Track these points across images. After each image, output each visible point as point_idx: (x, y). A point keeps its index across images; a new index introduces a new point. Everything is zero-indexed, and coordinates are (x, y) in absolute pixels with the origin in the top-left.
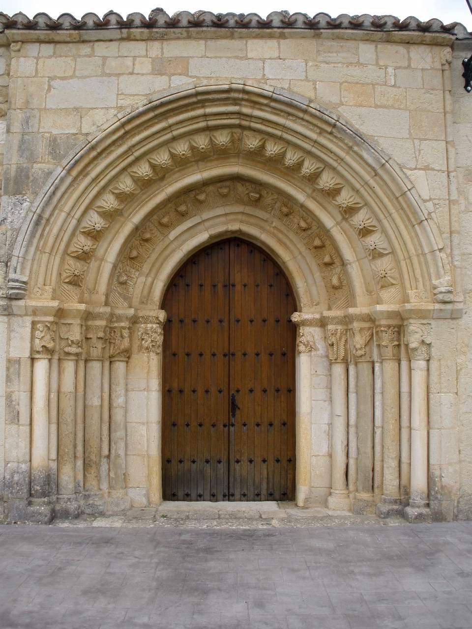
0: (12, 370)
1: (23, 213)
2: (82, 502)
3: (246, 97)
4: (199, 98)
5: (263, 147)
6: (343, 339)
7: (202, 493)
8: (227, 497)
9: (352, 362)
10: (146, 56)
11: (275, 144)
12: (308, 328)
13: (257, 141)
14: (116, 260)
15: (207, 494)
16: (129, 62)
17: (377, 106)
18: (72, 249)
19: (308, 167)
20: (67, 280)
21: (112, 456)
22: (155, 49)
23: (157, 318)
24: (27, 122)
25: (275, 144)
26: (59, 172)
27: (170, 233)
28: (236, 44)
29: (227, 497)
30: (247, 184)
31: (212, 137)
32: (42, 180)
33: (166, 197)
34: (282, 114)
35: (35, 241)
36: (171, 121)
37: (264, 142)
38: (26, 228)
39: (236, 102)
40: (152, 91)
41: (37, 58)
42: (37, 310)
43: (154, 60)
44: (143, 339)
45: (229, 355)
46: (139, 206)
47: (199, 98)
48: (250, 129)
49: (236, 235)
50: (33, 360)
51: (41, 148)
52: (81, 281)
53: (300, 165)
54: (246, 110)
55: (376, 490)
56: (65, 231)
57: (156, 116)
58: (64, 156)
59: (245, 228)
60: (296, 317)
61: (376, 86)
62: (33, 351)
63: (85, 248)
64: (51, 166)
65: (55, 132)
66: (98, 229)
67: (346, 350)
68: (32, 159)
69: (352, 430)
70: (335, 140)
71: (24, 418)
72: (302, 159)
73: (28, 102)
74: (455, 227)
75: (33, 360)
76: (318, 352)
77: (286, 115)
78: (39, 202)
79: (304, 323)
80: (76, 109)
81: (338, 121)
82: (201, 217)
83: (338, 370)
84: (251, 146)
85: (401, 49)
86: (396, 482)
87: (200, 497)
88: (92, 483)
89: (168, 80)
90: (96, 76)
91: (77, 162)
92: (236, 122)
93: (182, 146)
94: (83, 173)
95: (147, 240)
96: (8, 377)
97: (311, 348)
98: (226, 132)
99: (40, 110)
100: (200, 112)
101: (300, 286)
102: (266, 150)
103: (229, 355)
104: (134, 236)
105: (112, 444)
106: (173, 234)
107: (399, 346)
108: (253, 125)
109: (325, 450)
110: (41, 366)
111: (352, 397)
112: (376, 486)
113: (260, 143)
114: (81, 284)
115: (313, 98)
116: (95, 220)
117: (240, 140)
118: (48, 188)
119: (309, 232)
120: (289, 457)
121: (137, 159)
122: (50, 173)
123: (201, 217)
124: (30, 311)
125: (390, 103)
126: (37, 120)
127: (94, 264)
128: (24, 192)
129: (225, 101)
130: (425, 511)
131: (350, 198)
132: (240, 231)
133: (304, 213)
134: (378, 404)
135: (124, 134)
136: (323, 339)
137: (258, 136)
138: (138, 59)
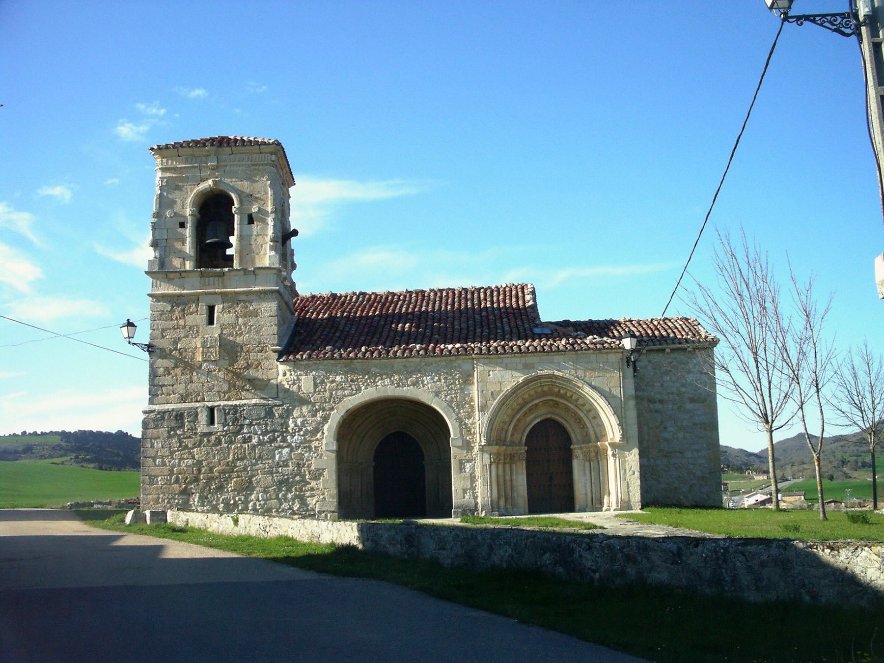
10: (520, 363)
16: (514, 365)
19: (574, 397)
22: (523, 360)
23: (525, 449)
28: (550, 358)
39: (551, 378)
43: (523, 365)
45: (548, 461)
50: (490, 465)
53: (572, 397)
54: (553, 380)
59: (553, 416)
60: (572, 447)
62: (491, 462)
74: (623, 416)
83: (587, 464)
85: (605, 355)
97: (577, 457)
101: (572, 435)
103: (548, 461)
109: (584, 492)
117: (552, 388)
129: (547, 378)
134: (601, 475)
138: (518, 364)
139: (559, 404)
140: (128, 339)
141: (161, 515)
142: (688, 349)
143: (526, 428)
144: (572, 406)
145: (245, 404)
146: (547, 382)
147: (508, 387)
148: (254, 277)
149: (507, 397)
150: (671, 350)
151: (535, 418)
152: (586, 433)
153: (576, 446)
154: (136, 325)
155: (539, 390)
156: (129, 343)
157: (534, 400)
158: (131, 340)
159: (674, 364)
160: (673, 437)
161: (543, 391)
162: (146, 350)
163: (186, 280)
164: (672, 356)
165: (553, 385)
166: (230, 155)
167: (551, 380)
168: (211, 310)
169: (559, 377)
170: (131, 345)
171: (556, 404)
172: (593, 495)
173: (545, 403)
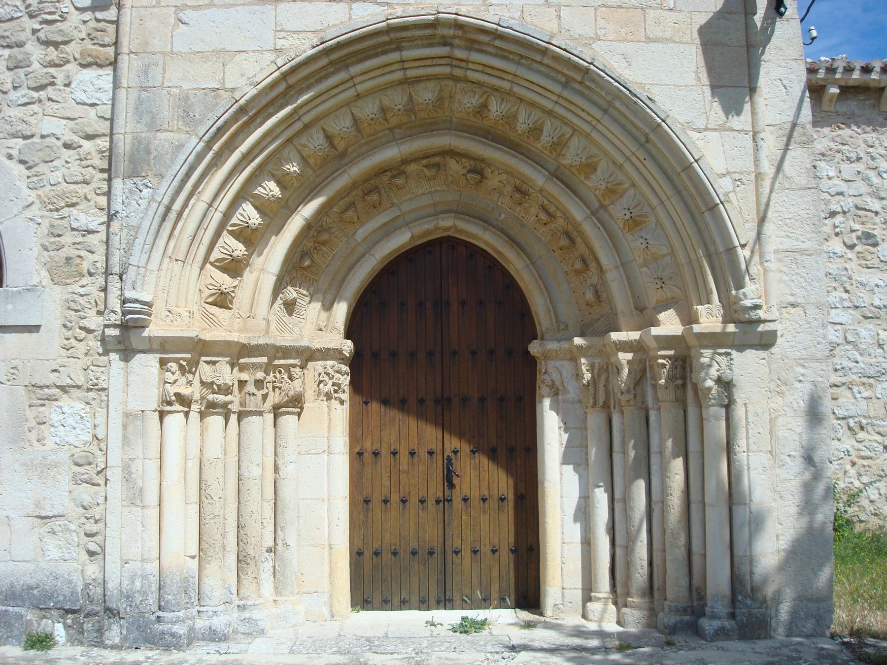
0: (130, 428)
2: (236, 614)
3: (459, 33)
4: (393, 36)
5: (485, 106)
6: (603, 377)
7: (407, 598)
8: (442, 604)
9: (617, 409)
11: (503, 100)
12: (552, 362)
13: (477, 97)
14: (281, 270)
15: (415, 599)
17: (649, 40)
18: (216, 255)
20: (210, 300)
21: (280, 547)
24: (146, 72)
25: (503, 100)
26: (194, 145)
27: (356, 232)
29: (442, 604)
30: (464, 160)
31: (413, 94)
32: (169, 156)
33: (350, 181)
34: (511, 56)
35: (161, 242)
36: (355, 69)
37: (487, 99)
38: (148, 223)
39: (445, 42)
40: (325, 25)
42: (167, 343)
44: (321, 382)
46: (312, 194)
47: (393, 36)
48: (466, 80)
49: (449, 233)
50: (162, 415)
51: (167, 112)
52: (231, 303)
53: (536, 131)
54: (459, 54)
55: (656, 594)
56: (206, 230)
57: (331, 63)
58: (201, 122)
59: (462, 225)
60: (534, 348)
61: (647, 11)
63: (235, 254)
64: (183, 136)
65: (186, 86)
66: (254, 227)
67: (607, 393)
68: (155, 127)
70: (586, 92)
71: (152, 498)
72: (541, 121)
73: (146, 43)
75: (162, 415)
76: (568, 396)
77: (517, 58)
78: (165, 189)
79: (546, 356)
80: (219, 52)
81: (591, 64)
82: (400, 209)
83: (595, 420)
84: (468, 105)
86: (684, 582)
87: (404, 605)
88: (249, 588)
89: (347, 10)
90: (243, 5)
91: (220, 131)
92: (447, 70)
93: (371, 106)
94: (230, 146)
95: (324, 243)
96: (125, 437)
98: (431, 85)
99: (163, 54)
100: (395, 56)
101: (538, 304)
102: (489, 111)
104: (306, 237)
105: (279, 530)
106: (361, 234)
107: (684, 386)
108: (471, 75)
112: (655, 587)
113: (481, 101)
114: (230, 306)
115: (556, 30)
116: (249, 214)
118: (178, 168)
119: (553, 226)
120: (529, 545)
121: (307, 127)
122: (181, 146)
123: (400, 209)
124: (156, 346)
125: (668, 34)
126: (159, 70)
127: (249, 276)
128: (144, 174)
130: (728, 624)
131: (610, 176)
133: (545, 200)
135: (287, 89)
136: (574, 377)
137: (478, 90)
139: (488, 172)
144: (538, 178)
150: (840, 87)
151: (387, 230)
152: (597, 293)
153: (552, 346)
155: (396, 99)
157: (374, 144)
160: (846, 338)
161: (411, 108)
165: (456, 79)
169: (483, 38)
172: (619, 551)
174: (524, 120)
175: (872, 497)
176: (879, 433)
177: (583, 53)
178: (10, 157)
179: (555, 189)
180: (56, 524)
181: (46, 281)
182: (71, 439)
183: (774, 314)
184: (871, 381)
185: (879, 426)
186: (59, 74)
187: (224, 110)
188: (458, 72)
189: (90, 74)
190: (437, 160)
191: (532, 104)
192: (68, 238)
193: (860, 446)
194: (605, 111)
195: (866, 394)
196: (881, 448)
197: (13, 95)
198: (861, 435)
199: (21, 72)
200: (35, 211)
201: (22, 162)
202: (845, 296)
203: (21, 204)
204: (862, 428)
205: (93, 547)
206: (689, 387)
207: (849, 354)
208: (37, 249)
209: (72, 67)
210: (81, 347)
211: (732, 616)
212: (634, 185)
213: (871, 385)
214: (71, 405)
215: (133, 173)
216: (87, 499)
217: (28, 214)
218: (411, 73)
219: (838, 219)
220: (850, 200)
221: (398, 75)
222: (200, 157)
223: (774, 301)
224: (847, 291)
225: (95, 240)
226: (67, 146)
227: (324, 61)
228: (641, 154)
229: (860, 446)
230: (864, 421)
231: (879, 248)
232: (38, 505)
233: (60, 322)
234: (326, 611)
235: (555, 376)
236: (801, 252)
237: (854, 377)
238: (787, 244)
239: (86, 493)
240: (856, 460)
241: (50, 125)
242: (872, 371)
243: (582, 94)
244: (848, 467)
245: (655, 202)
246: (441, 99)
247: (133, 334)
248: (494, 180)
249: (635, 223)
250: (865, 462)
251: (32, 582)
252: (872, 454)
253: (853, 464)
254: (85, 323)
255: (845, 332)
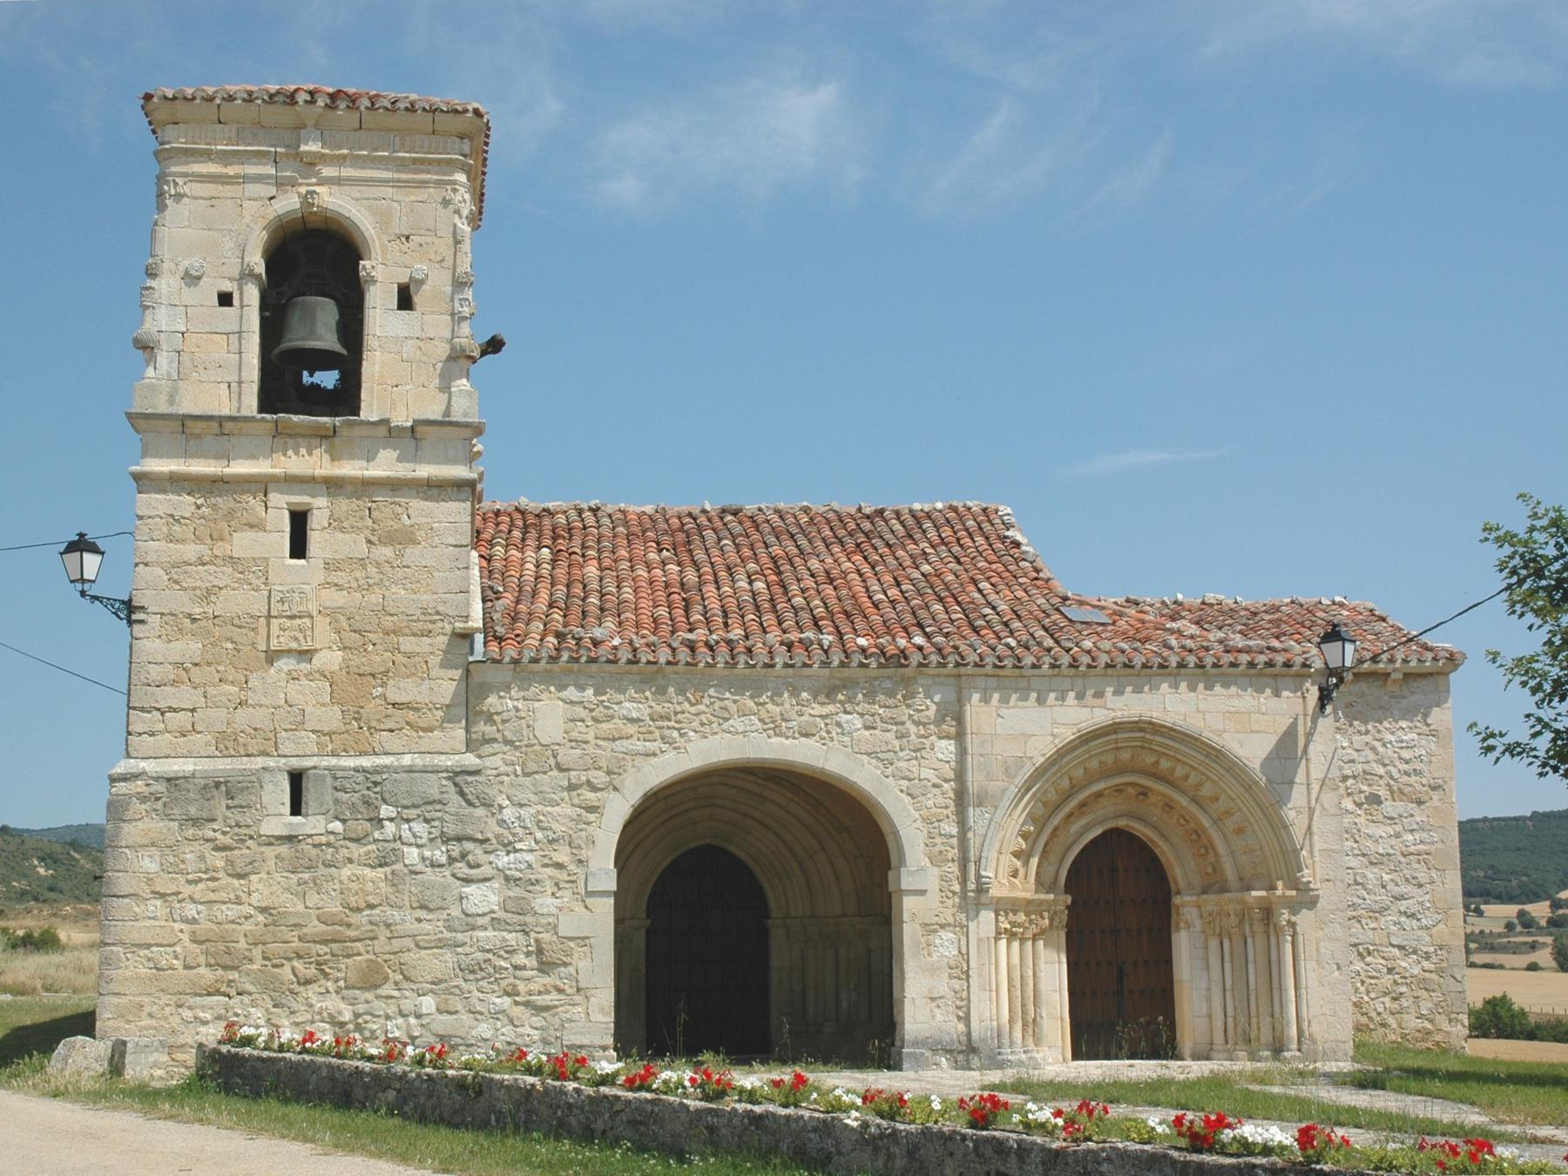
1: (986, 822)
17: (1252, 732)
19: (1193, 779)
39: (1142, 730)
41: (985, 690)
50: (996, 939)
53: (1186, 777)
54: (1148, 736)
59: (1131, 824)
62: (998, 933)
64: (1006, 784)
67: (1221, 928)
69: (1228, 994)
79: (1183, 905)
83: (1214, 943)
97: (1188, 926)
99: (991, 735)
100: (1114, 737)
107: (1268, 924)
110: (1003, 943)
111: (1227, 966)
122: (1005, 789)
125: (1262, 728)
132: (1127, 826)
139: (1150, 794)
140: (79, 586)
141: (157, 1050)
142: (1394, 676)
143: (1068, 849)
144: (1184, 802)
145: (386, 766)
146: (1134, 739)
147: (1041, 749)
148: (413, 443)
149: (1040, 773)
151: (1088, 828)
153: (1187, 898)
154: (102, 550)
155: (1109, 759)
156: (83, 593)
157: (1091, 783)
158: (86, 587)
159: (1359, 708)
161: (1116, 760)
162: (122, 616)
163: (233, 440)
164: (1356, 688)
166: (355, 130)
167: (1142, 734)
168: (299, 521)
169: (1163, 730)
170: (86, 602)
171: (1144, 793)
173: (1118, 790)
174: (1180, 771)
175: (1379, 1010)
176: (1383, 958)
177: (1217, 741)
178: (902, 791)
179: (1193, 809)
180: (940, 1002)
181: (929, 864)
182: (947, 954)
183: (1318, 885)
184: (1376, 915)
185: (1382, 951)
186: (927, 742)
187: (1028, 770)
188: (1146, 745)
189: (944, 743)
190: (1121, 787)
191: (1185, 763)
192: (938, 840)
193: (1368, 968)
194: (1227, 771)
195: (1372, 926)
196: (1385, 971)
197: (901, 754)
198: (1369, 959)
199: (905, 740)
200: (919, 824)
201: (909, 794)
202: (1355, 846)
203: (912, 819)
204: (1369, 954)
205: (961, 1014)
206: (1272, 927)
207: (1358, 893)
208: (922, 845)
209: (933, 738)
210: (950, 902)
211: (1299, 1050)
212: (1240, 810)
213: (1376, 919)
214: (947, 935)
215: (980, 804)
216: (957, 987)
217: (915, 825)
218: (1119, 745)
219: (1351, 781)
220: (1360, 766)
221: (1113, 746)
222: (1016, 795)
223: (1318, 878)
224: (1356, 842)
225: (954, 841)
226: (935, 786)
227: (1078, 741)
228: (1247, 795)
229: (1368, 968)
230: (1371, 948)
231: (1383, 806)
232: (930, 991)
233: (937, 888)
234: (1061, 1058)
235: (1189, 917)
236: (1333, 851)
237: (1363, 912)
238: (1325, 846)
239: (957, 984)
240: (1365, 979)
241: (926, 773)
242: (1377, 907)
243: (1214, 761)
244: (1359, 985)
245: (1253, 820)
246: (1133, 757)
247: (983, 894)
248: (1153, 799)
249: (1239, 831)
250: (1373, 981)
251: (928, 1035)
252: (1378, 975)
253: (1363, 982)
254: (952, 888)
255: (1355, 874)
